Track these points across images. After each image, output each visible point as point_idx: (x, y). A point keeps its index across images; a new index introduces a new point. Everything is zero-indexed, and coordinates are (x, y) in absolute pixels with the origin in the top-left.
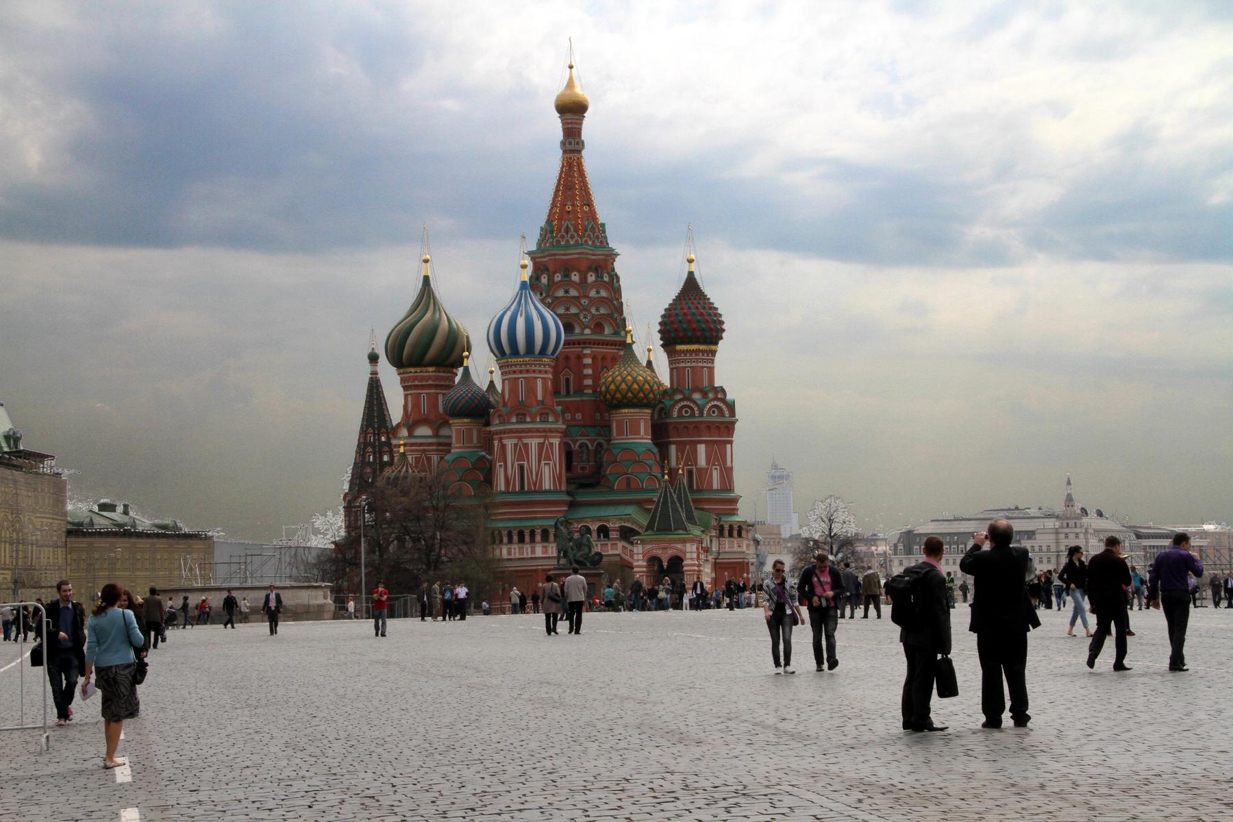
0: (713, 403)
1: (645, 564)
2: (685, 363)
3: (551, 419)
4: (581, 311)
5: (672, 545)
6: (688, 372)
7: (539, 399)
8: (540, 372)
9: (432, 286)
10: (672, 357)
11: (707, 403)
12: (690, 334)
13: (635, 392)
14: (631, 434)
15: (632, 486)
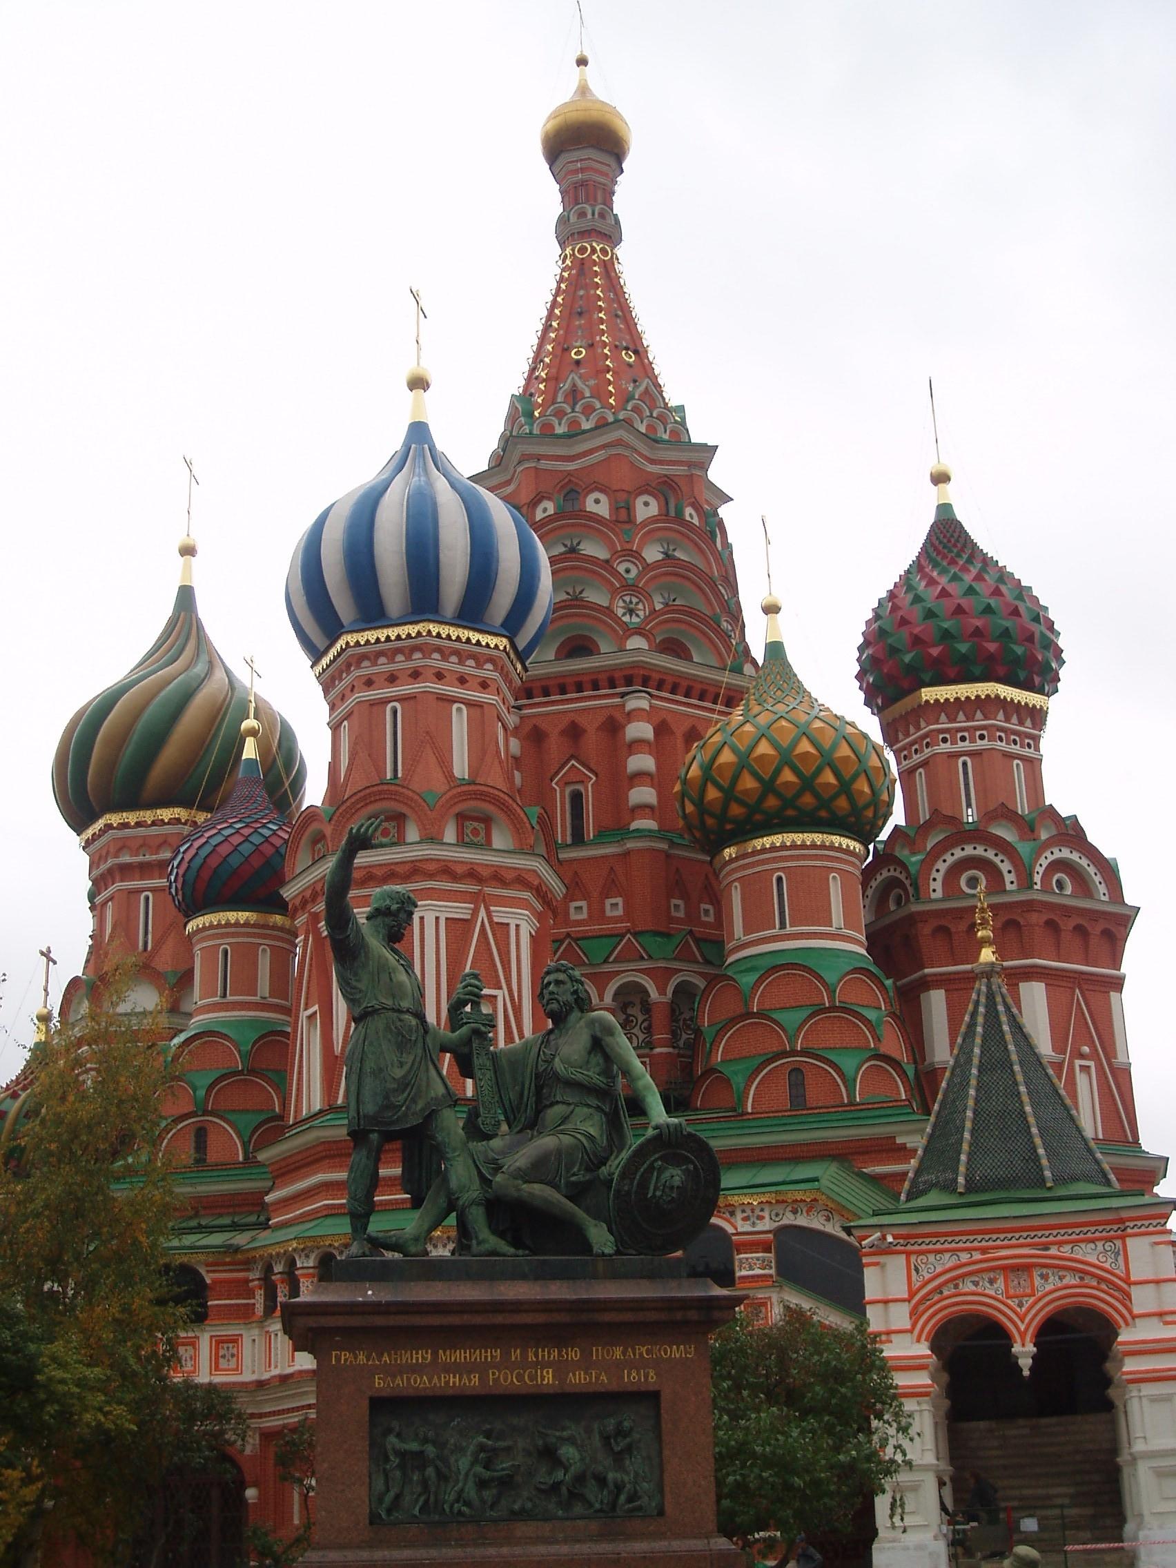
0: (1058, 855)
1: (923, 1349)
2: (954, 743)
3: (501, 839)
4: (614, 592)
5: (1053, 1251)
6: (965, 775)
7: (457, 773)
8: (462, 680)
9: (201, 615)
10: (907, 735)
11: (1038, 853)
12: (963, 648)
13: (807, 771)
14: (791, 926)
15: (814, 1093)
